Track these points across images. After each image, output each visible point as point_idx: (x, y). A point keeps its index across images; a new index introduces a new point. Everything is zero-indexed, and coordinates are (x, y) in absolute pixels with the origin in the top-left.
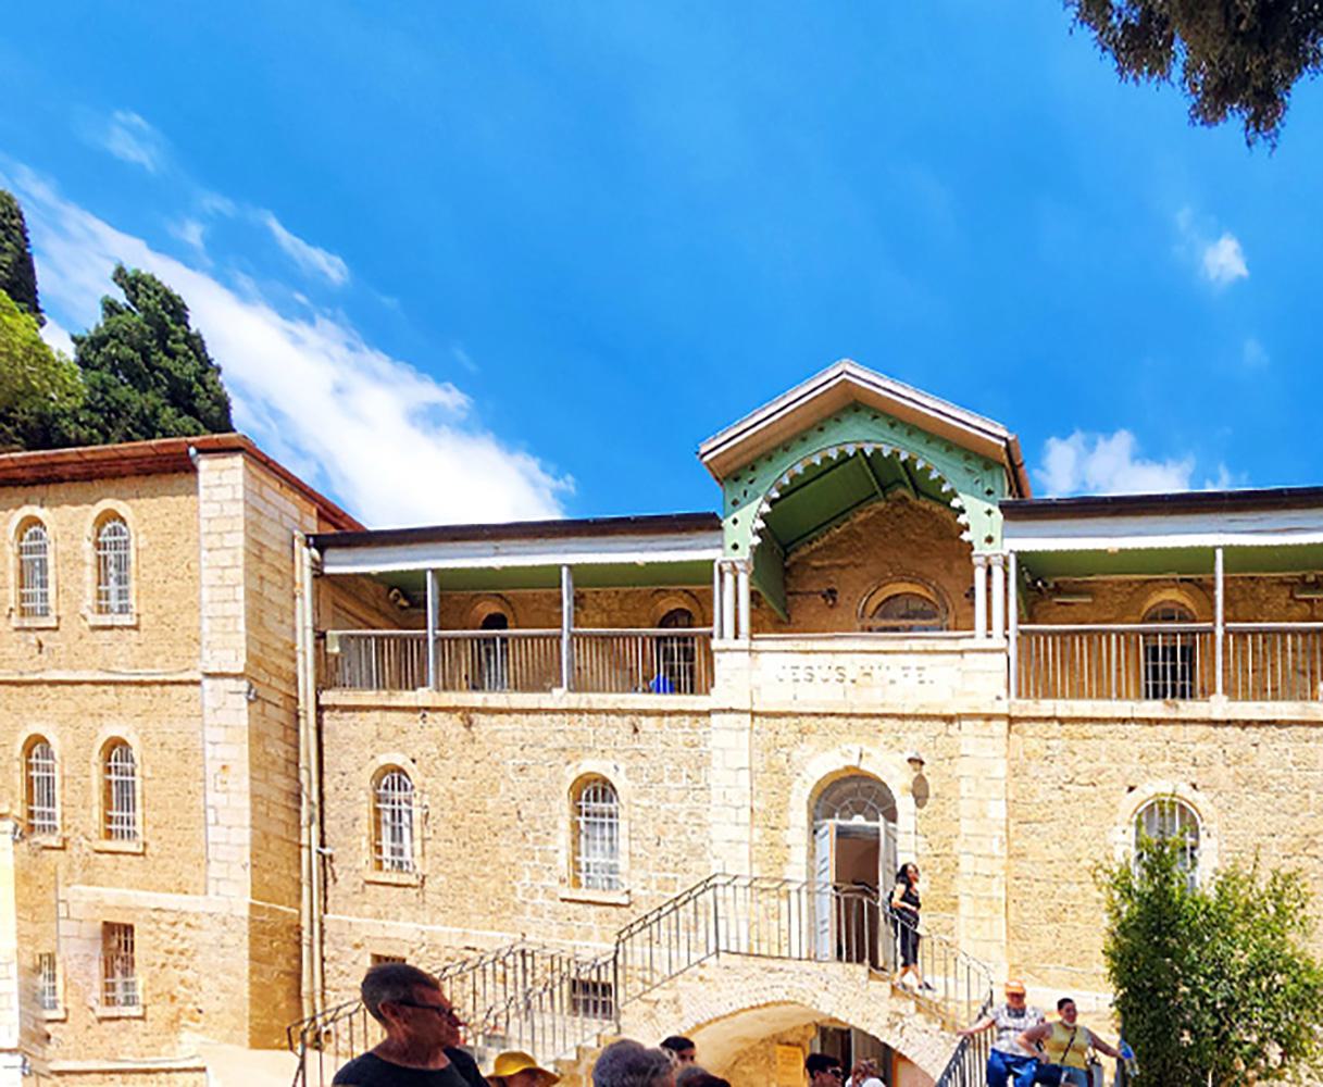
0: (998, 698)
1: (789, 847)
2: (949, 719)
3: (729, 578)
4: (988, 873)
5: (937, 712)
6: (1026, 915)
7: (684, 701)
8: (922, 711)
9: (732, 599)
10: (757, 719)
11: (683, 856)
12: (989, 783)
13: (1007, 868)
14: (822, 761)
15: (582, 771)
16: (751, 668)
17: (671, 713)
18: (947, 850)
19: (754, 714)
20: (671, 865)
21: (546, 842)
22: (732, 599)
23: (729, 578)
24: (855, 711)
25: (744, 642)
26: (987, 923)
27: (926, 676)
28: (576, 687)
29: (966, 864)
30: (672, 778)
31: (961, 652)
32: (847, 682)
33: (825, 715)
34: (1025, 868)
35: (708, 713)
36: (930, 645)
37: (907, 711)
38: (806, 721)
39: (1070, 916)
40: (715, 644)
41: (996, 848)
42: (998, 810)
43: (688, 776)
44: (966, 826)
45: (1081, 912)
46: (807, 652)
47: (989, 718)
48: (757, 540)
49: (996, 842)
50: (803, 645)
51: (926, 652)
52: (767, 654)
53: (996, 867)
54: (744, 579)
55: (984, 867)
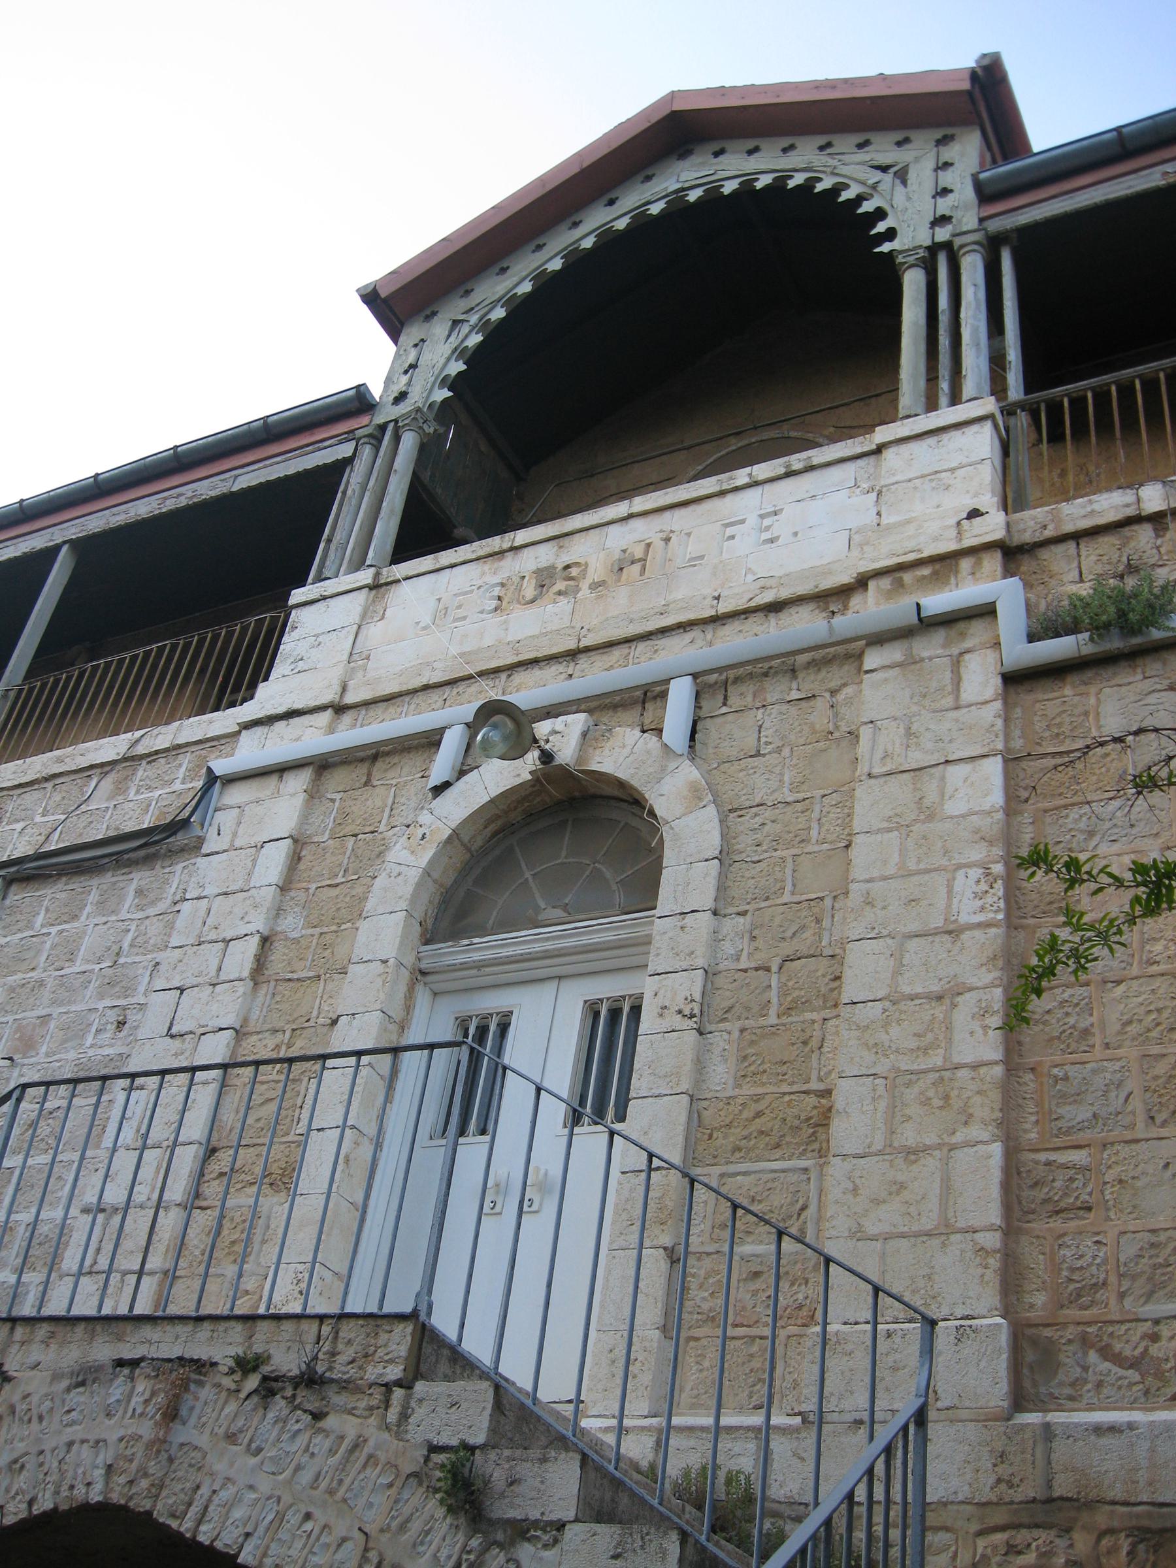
4: (936, 988)
8: (768, 597)
24: (584, 643)
26: (931, 1163)
27: (781, 527)
29: (866, 970)
31: (879, 450)
32: (584, 592)
37: (724, 608)
46: (501, 553)
49: (967, 882)
55: (927, 967)
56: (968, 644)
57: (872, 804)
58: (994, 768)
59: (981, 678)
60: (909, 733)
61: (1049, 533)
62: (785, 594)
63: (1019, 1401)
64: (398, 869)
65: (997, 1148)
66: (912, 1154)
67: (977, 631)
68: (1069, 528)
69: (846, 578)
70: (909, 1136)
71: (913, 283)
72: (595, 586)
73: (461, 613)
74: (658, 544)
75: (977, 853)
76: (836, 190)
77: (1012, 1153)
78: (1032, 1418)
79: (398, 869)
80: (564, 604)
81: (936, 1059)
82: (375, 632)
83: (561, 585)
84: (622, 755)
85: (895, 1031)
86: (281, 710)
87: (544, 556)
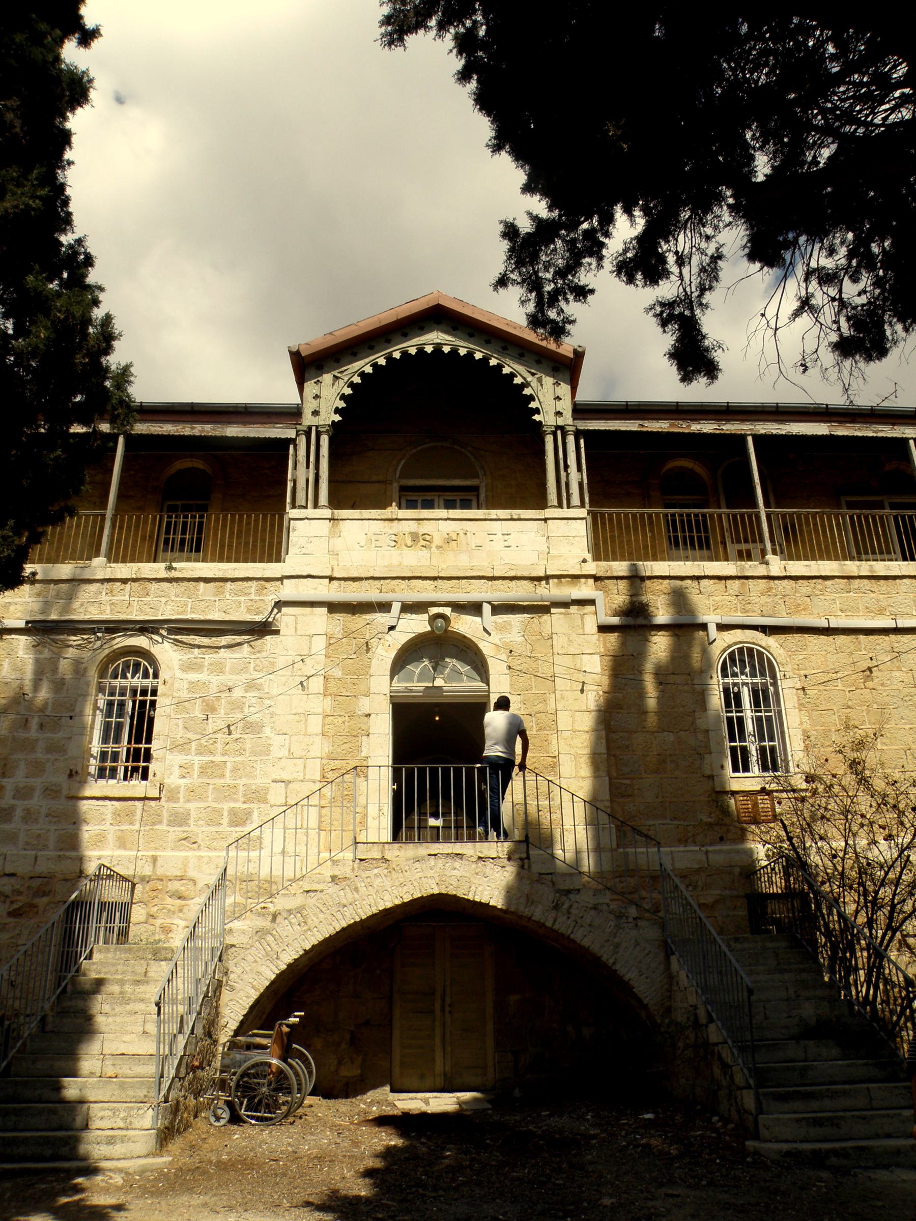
0: (584, 561)
5: (526, 574)
10: (335, 582)
17: (234, 580)
18: (541, 707)
19: (331, 579)
20: (219, 746)
24: (441, 575)
27: (511, 540)
32: (434, 549)
33: (410, 578)
35: (281, 579)
37: (496, 575)
48: (337, 418)
51: (512, 519)
56: (585, 611)
59: (591, 626)
60: (569, 640)
61: (609, 574)
62: (519, 574)
63: (618, 846)
64: (381, 658)
65: (607, 778)
67: (590, 609)
68: (615, 574)
69: (542, 574)
71: (549, 439)
72: (438, 547)
73: (378, 544)
74: (461, 534)
76: (531, 398)
77: (610, 779)
78: (621, 850)
79: (381, 658)
80: (425, 551)
82: (338, 543)
83: (424, 543)
84: (465, 625)
85: (575, 741)
86: (305, 574)
87: (412, 526)
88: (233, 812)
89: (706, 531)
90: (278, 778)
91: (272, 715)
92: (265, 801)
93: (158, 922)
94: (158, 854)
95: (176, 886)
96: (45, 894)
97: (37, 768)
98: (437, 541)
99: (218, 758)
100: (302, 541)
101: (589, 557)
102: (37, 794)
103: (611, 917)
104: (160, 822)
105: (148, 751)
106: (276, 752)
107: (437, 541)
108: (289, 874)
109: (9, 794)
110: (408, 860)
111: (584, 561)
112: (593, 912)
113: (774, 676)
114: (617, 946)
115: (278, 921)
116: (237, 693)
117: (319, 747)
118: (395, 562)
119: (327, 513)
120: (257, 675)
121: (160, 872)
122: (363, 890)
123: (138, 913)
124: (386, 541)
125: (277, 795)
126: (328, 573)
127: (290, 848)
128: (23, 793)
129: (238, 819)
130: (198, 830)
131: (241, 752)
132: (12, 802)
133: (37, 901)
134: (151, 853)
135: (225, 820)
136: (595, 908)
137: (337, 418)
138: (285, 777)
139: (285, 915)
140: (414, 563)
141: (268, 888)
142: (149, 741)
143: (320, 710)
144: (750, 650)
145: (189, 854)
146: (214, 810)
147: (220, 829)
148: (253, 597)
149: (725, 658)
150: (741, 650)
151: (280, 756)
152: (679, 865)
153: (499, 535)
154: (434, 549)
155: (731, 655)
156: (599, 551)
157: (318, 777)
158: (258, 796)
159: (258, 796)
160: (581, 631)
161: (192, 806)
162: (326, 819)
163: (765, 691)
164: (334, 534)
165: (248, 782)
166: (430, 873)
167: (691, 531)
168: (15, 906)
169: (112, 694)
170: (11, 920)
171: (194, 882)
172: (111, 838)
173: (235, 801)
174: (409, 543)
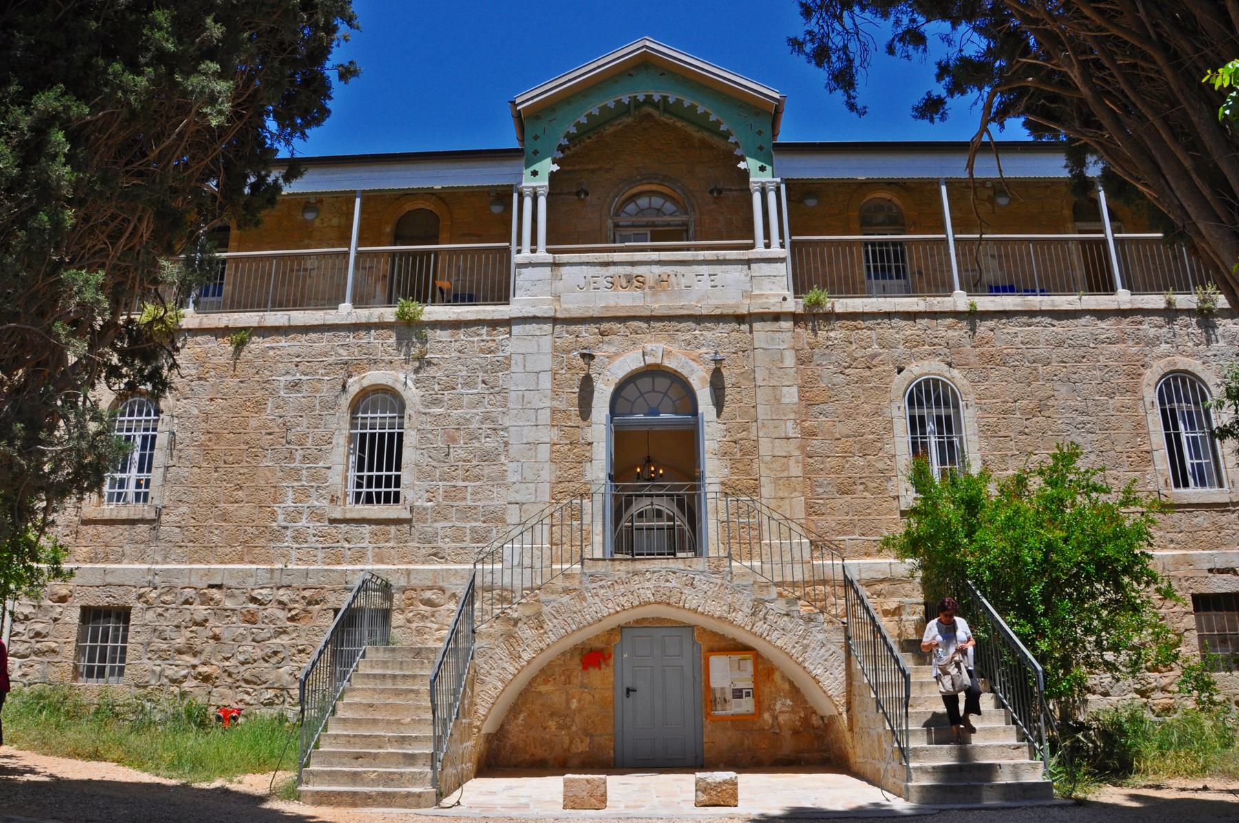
1: (590, 444)
2: (740, 319)
3: (528, 202)
5: (731, 312)
6: (820, 490)
7: (478, 312)
8: (718, 312)
9: (531, 214)
11: (475, 463)
12: (779, 373)
13: (802, 448)
14: (619, 361)
15: (366, 383)
16: (546, 282)
21: (316, 460)
22: (531, 214)
23: (528, 202)
25: (542, 255)
28: (360, 301)
29: (765, 447)
30: (466, 385)
31: (748, 262)
32: (647, 290)
34: (816, 443)
36: (722, 254)
37: (704, 312)
38: (605, 326)
39: (862, 487)
40: (516, 258)
41: (791, 429)
42: (791, 395)
43: (484, 382)
44: (762, 412)
45: (869, 483)
46: (607, 264)
47: (776, 317)
49: (790, 424)
50: (604, 257)
52: (568, 268)
53: (792, 448)
54: (542, 202)
55: (781, 449)
57: (761, 395)
58: (795, 389)
66: (782, 498)
70: (781, 494)
75: (792, 416)
80: (639, 292)
81: (785, 474)
87: (628, 270)
88: (473, 530)
89: (903, 261)
90: (513, 500)
91: (506, 444)
92: (503, 521)
93: (414, 625)
94: (411, 567)
95: (428, 594)
96: (317, 603)
97: (304, 492)
98: (650, 281)
99: (461, 484)
100: (527, 285)
101: (789, 294)
102: (304, 517)
103: (801, 622)
104: (413, 540)
105: (398, 478)
106: (512, 477)
107: (650, 281)
108: (527, 584)
109: (281, 517)
110: (628, 572)
111: (785, 299)
112: (786, 618)
113: (956, 406)
114: (806, 647)
115: (519, 625)
116: (474, 426)
117: (548, 473)
118: (612, 303)
119: (549, 258)
120: (490, 408)
121: (413, 582)
122: (590, 600)
123: (397, 619)
124: (603, 282)
125: (513, 516)
126: (551, 314)
127: (527, 562)
128: (294, 515)
129: (479, 537)
130: (446, 547)
131: (478, 478)
132: (284, 524)
133: (310, 608)
134: (404, 567)
135: (468, 539)
136: (788, 615)
137: (556, 168)
138: (519, 498)
139: (524, 620)
140: (629, 303)
141: (505, 596)
142: (399, 468)
143: (547, 440)
144: (936, 381)
145: (438, 567)
146: (458, 528)
147: (463, 545)
148: (485, 337)
149: (912, 391)
150: (927, 381)
151: (514, 480)
152: (864, 576)
153: (706, 275)
154: (647, 290)
155: (918, 385)
156: (799, 288)
157: (547, 498)
158: (496, 517)
159: (496, 517)
160: (780, 365)
161: (438, 525)
162: (557, 536)
163: (948, 418)
164: (555, 277)
165: (487, 503)
166: (647, 585)
167: (889, 261)
168: (293, 613)
169: (364, 426)
170: (289, 624)
171: (443, 590)
172: (370, 554)
173: (476, 520)
174: (624, 285)
